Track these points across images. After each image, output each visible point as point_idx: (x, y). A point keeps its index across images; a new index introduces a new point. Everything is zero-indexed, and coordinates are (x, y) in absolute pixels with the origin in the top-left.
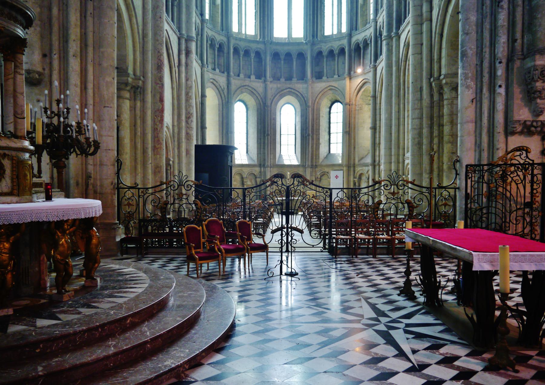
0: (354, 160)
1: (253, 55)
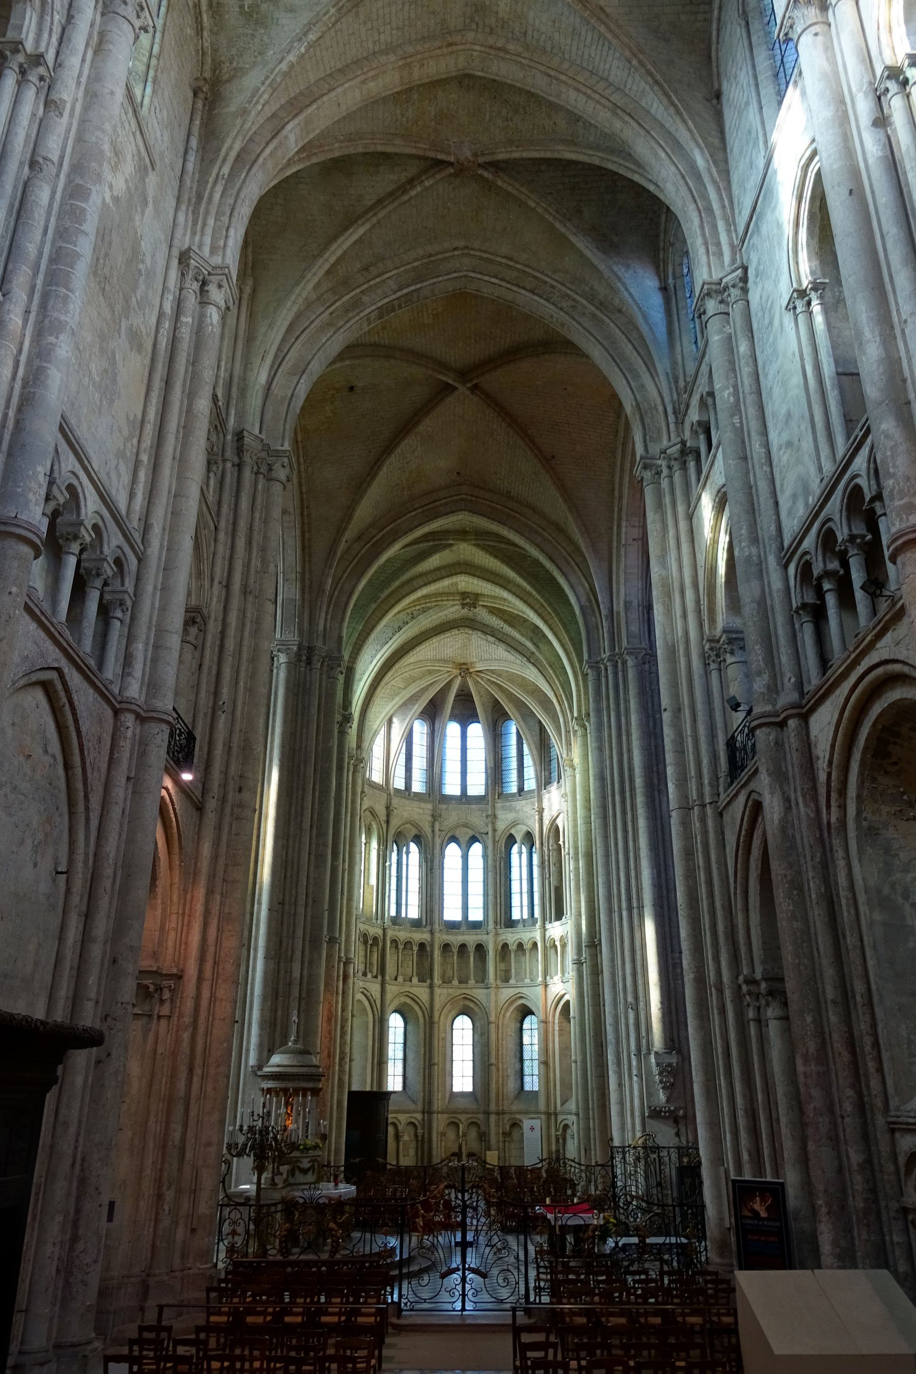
1: (415, 948)
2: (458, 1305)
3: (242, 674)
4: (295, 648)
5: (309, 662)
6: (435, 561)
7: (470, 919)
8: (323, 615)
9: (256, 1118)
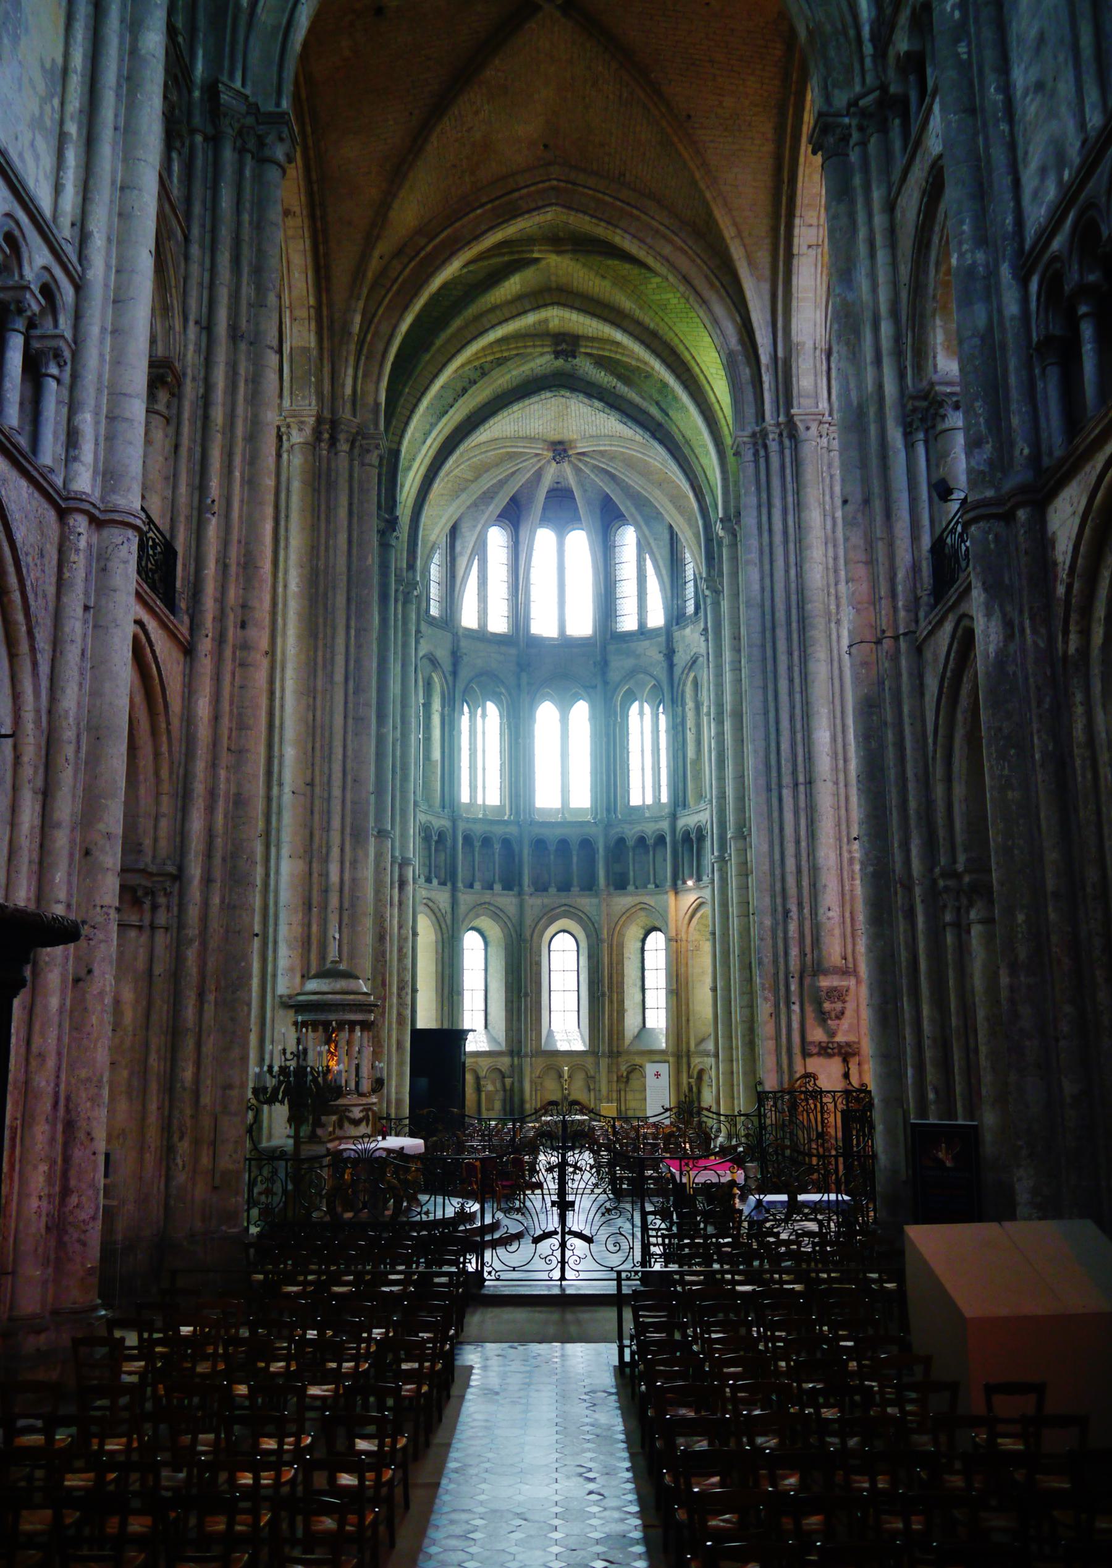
0: (688, 1043)
2: (557, 1274)
3: (238, 460)
4: (311, 421)
5: (333, 441)
6: (513, 285)
7: (572, 805)
8: (350, 371)
9: (289, 1056)
